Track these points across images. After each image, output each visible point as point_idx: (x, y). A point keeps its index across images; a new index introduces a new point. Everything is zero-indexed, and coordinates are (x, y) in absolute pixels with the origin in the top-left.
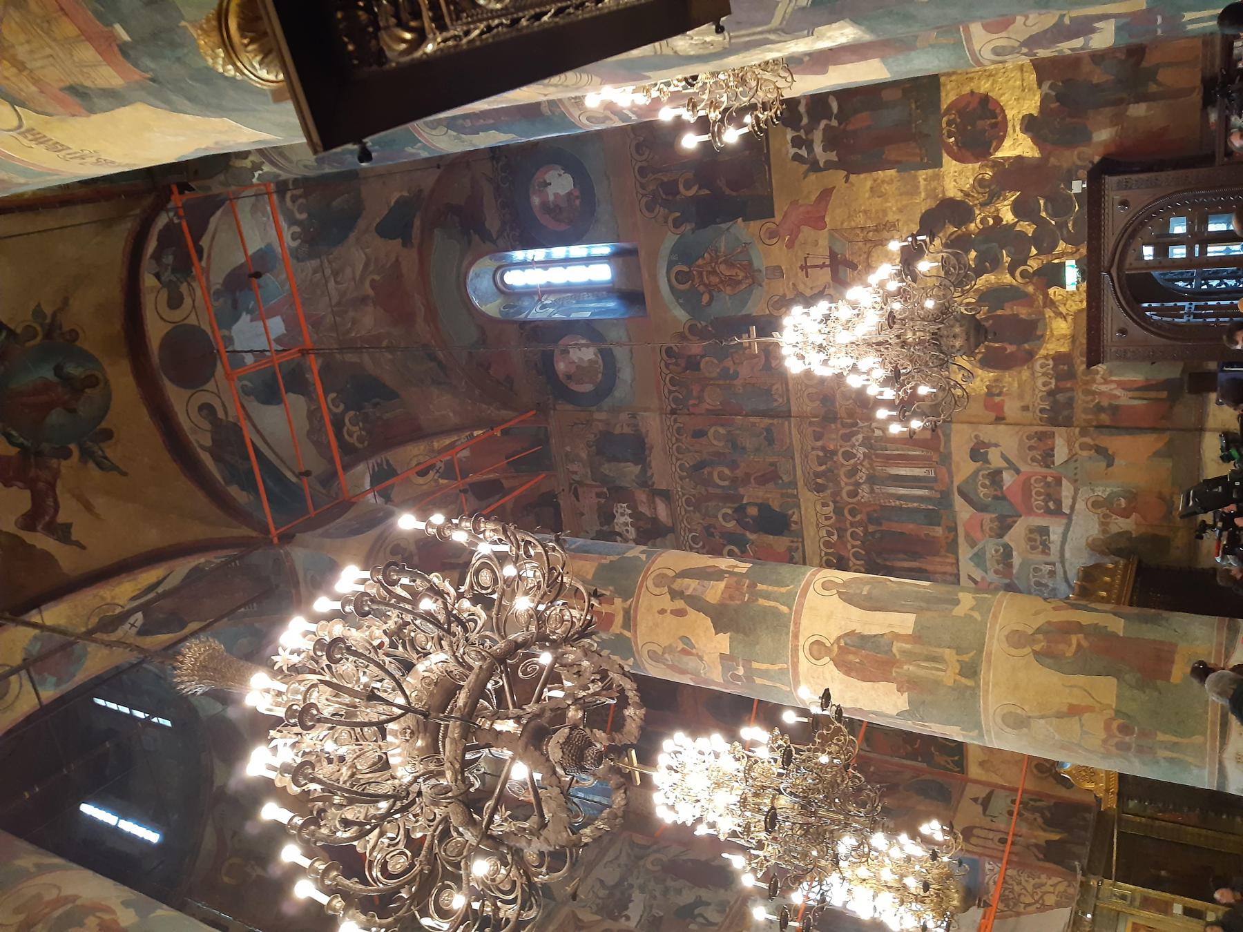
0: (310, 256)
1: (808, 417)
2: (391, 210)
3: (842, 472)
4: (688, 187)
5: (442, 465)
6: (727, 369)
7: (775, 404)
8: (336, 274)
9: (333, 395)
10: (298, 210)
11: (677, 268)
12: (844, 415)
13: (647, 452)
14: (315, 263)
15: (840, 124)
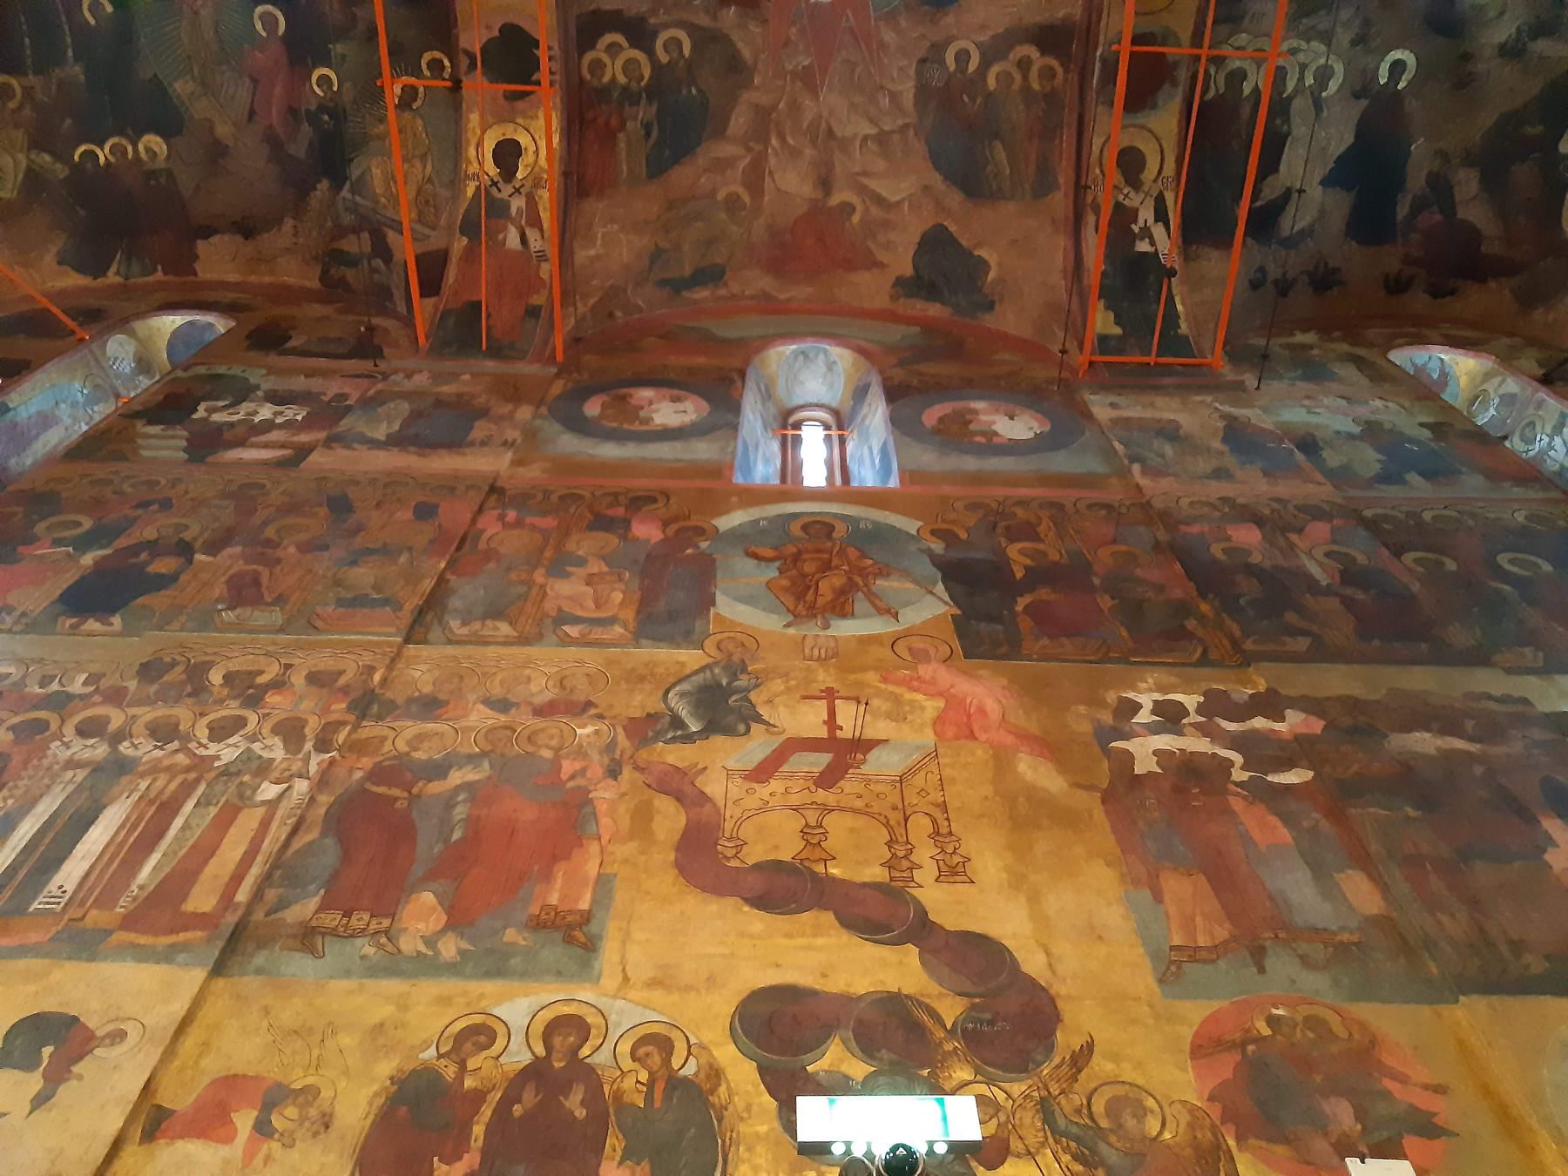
0: (922, 90)
1: (391, 665)
2: (966, 254)
3: (182, 713)
4: (1022, 552)
5: (504, 195)
6: (582, 562)
7: (454, 624)
8: (882, 139)
9: (687, 51)
10: (1004, 71)
11: (840, 530)
12: (363, 734)
13: (412, 449)
14: (908, 99)
15: (1240, 784)
